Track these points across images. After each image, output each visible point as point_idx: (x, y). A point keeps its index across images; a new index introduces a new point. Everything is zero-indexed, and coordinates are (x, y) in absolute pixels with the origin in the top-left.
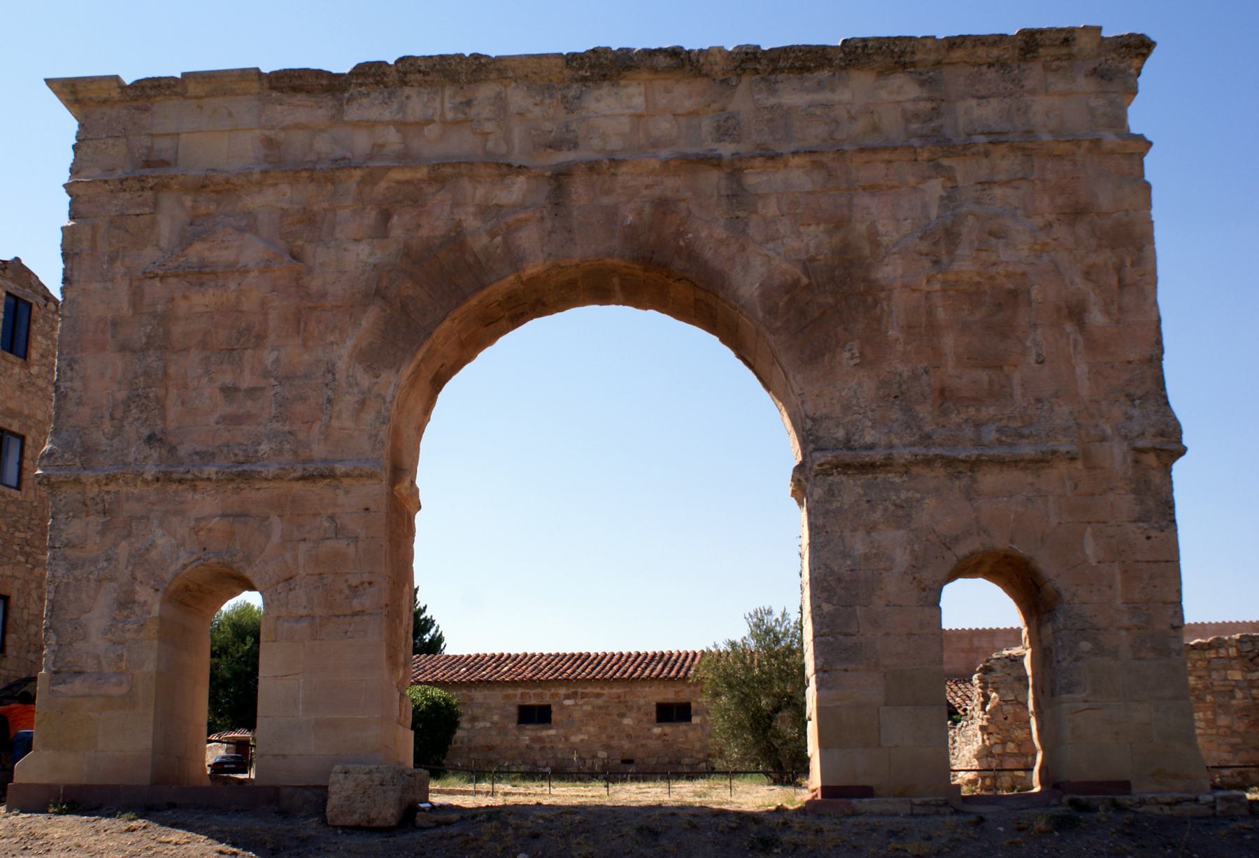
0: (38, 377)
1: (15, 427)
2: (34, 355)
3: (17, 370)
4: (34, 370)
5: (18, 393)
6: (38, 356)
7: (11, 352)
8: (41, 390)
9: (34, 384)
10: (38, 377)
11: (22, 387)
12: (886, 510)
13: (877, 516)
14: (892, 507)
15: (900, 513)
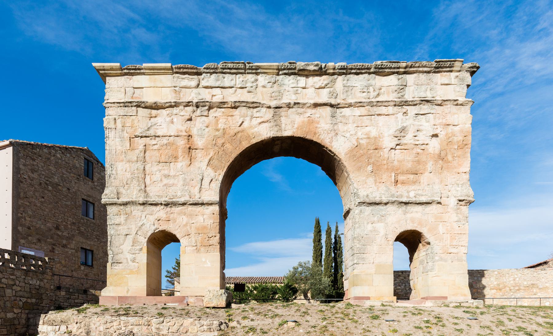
0: (97, 186)
1: (91, 200)
2: (95, 179)
3: (90, 183)
4: (96, 184)
5: (91, 190)
6: (97, 180)
7: (88, 177)
8: (98, 190)
9: (96, 188)
10: (97, 186)
11: (92, 188)
12: (378, 217)
13: (376, 219)
14: (380, 217)
15: (383, 218)
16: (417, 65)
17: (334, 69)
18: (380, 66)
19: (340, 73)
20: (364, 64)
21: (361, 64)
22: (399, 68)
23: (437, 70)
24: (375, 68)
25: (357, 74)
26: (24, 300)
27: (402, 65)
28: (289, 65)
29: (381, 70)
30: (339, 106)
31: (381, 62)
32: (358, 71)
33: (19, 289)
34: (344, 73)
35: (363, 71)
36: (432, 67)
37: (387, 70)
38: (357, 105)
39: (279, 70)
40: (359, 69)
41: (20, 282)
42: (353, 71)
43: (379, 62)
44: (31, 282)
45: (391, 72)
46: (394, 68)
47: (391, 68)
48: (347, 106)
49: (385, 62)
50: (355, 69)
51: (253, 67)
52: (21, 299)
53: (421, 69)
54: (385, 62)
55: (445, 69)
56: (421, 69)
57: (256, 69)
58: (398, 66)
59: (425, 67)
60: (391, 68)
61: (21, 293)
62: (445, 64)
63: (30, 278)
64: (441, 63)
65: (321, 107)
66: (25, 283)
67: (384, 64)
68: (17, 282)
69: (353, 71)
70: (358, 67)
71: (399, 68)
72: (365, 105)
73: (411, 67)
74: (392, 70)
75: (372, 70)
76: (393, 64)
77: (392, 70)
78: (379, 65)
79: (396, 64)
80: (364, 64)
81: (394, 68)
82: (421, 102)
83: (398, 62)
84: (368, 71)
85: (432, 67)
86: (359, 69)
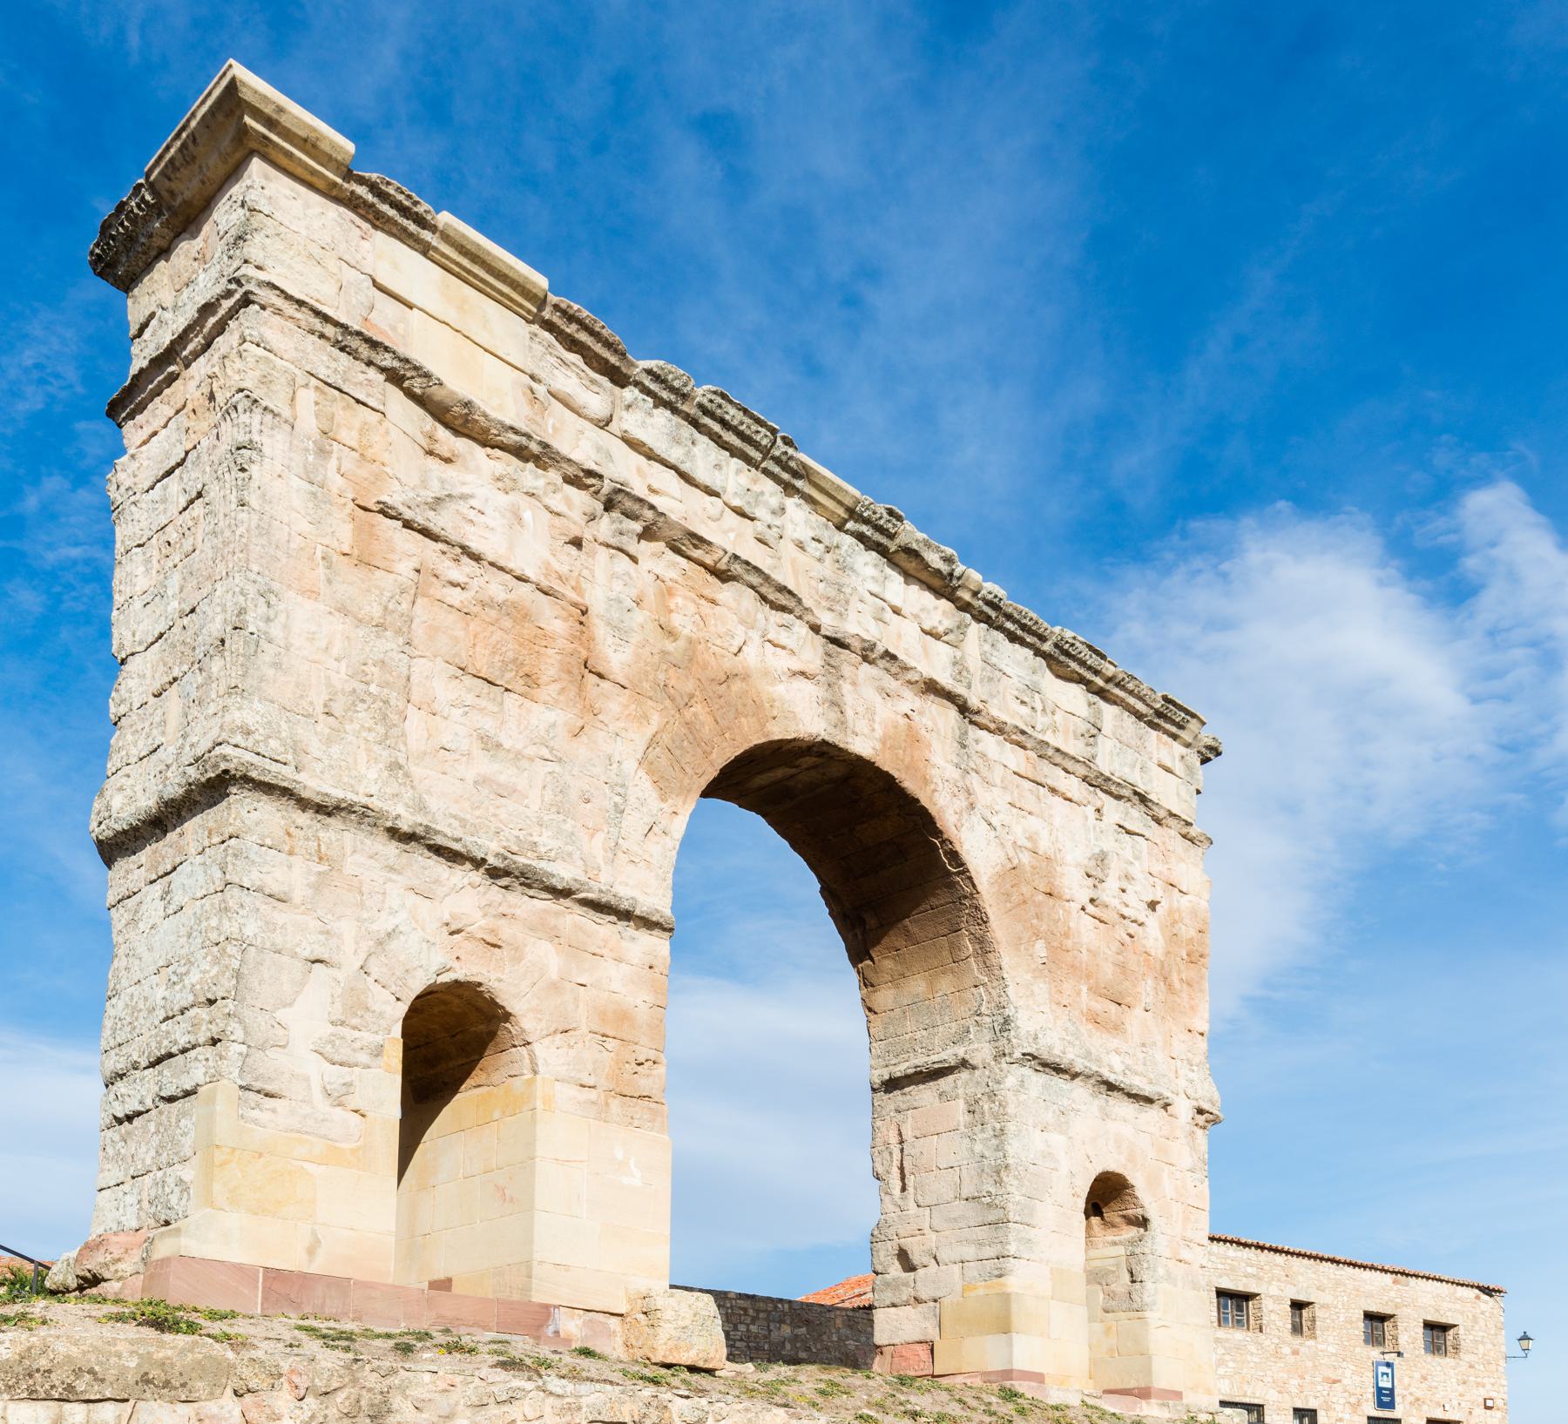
17: (975, 594)
18: (1066, 646)
19: (982, 612)
20: (1041, 621)
21: (1035, 616)
22: (1097, 672)
23: (1156, 720)
24: (1056, 645)
27: (1107, 669)
29: (1062, 658)
30: (976, 718)
31: (1073, 634)
32: (1019, 632)
34: (990, 617)
35: (1029, 639)
36: (1152, 708)
37: (1074, 665)
38: (1014, 737)
40: (1024, 627)
42: (1009, 625)
43: (1069, 634)
45: (1079, 674)
46: (1090, 668)
47: (1083, 663)
48: (992, 726)
49: (1081, 642)
50: (1015, 621)
53: (1132, 700)
54: (1081, 642)
55: (1168, 726)
56: (1132, 700)
58: (1099, 668)
60: (1083, 663)
62: (1175, 713)
64: (1171, 707)
65: (938, 700)
67: (1078, 644)
69: (1009, 625)
70: (1024, 621)
71: (1097, 672)
73: (1118, 685)
74: (1082, 671)
75: (1047, 647)
76: (1094, 656)
77: (1082, 671)
78: (1067, 642)
79: (1099, 658)
81: (1090, 668)
85: (1152, 708)
86: (1024, 627)
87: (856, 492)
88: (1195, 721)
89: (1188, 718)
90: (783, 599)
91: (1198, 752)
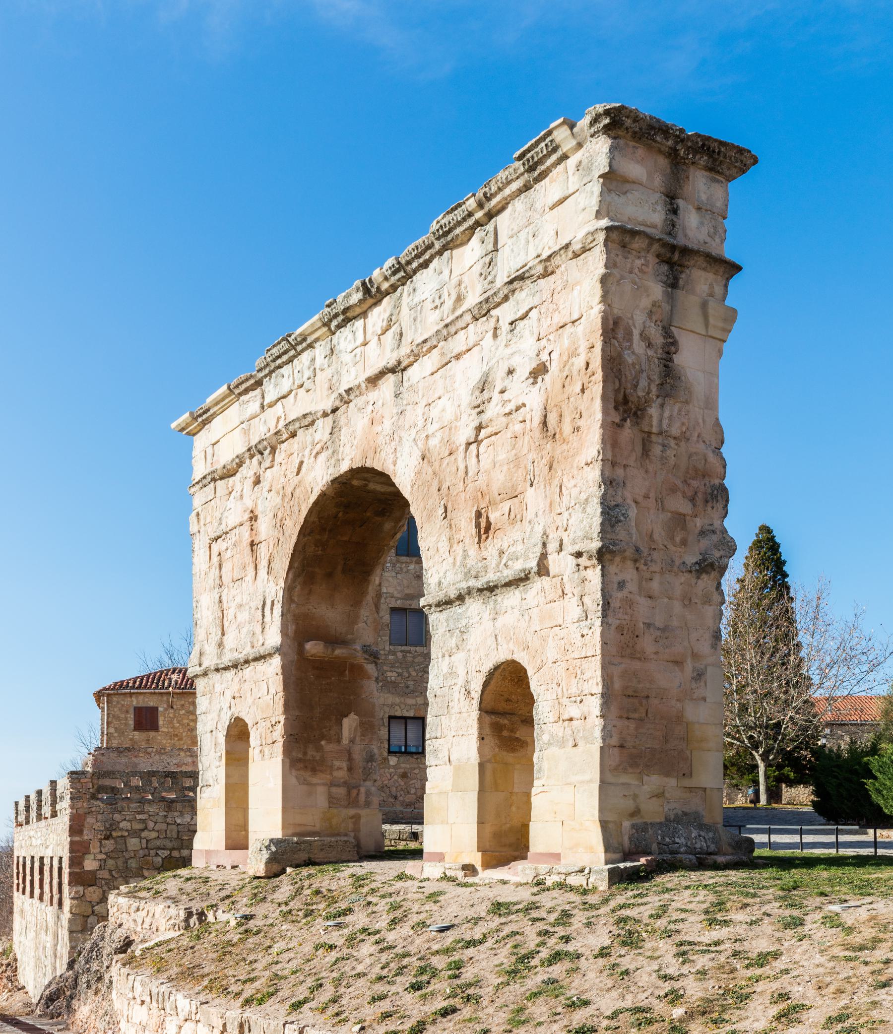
16: (494, 188)
17: (386, 279)
18: (441, 232)
19: (399, 280)
20: (417, 243)
21: (412, 246)
22: (470, 214)
23: (536, 174)
24: (438, 239)
25: (425, 265)
26: (164, 853)
27: (470, 206)
28: (329, 309)
29: (449, 237)
30: (403, 365)
31: (435, 222)
32: (421, 260)
33: (154, 835)
34: (403, 277)
35: (427, 256)
36: (522, 174)
37: (458, 231)
38: (424, 349)
39: (326, 324)
40: (418, 256)
41: (156, 823)
42: (415, 265)
43: (434, 226)
44: (179, 821)
45: (466, 230)
46: (464, 219)
47: (459, 223)
48: (412, 359)
49: (443, 218)
50: (413, 259)
51: (299, 339)
52: (160, 852)
53: (507, 191)
54: (443, 218)
55: (549, 162)
56: (507, 191)
57: (305, 340)
58: (466, 213)
59: (509, 182)
61: (158, 843)
62: (537, 153)
63: (176, 814)
64: (529, 155)
65: (383, 380)
66: (168, 824)
67: (442, 222)
68: (151, 825)
69: (415, 265)
70: (413, 255)
71: (470, 214)
72: (435, 343)
73: (488, 199)
74: (466, 225)
75: (437, 246)
76: (456, 212)
77: (466, 225)
78: (438, 230)
79: (459, 209)
80: (417, 243)
81: (464, 219)
82: (511, 287)
83: (460, 205)
84: (432, 251)
85: (522, 174)
86: (418, 256)
87: (316, 317)
88: (555, 133)
89: (550, 138)
90: (309, 419)
91: (592, 136)
